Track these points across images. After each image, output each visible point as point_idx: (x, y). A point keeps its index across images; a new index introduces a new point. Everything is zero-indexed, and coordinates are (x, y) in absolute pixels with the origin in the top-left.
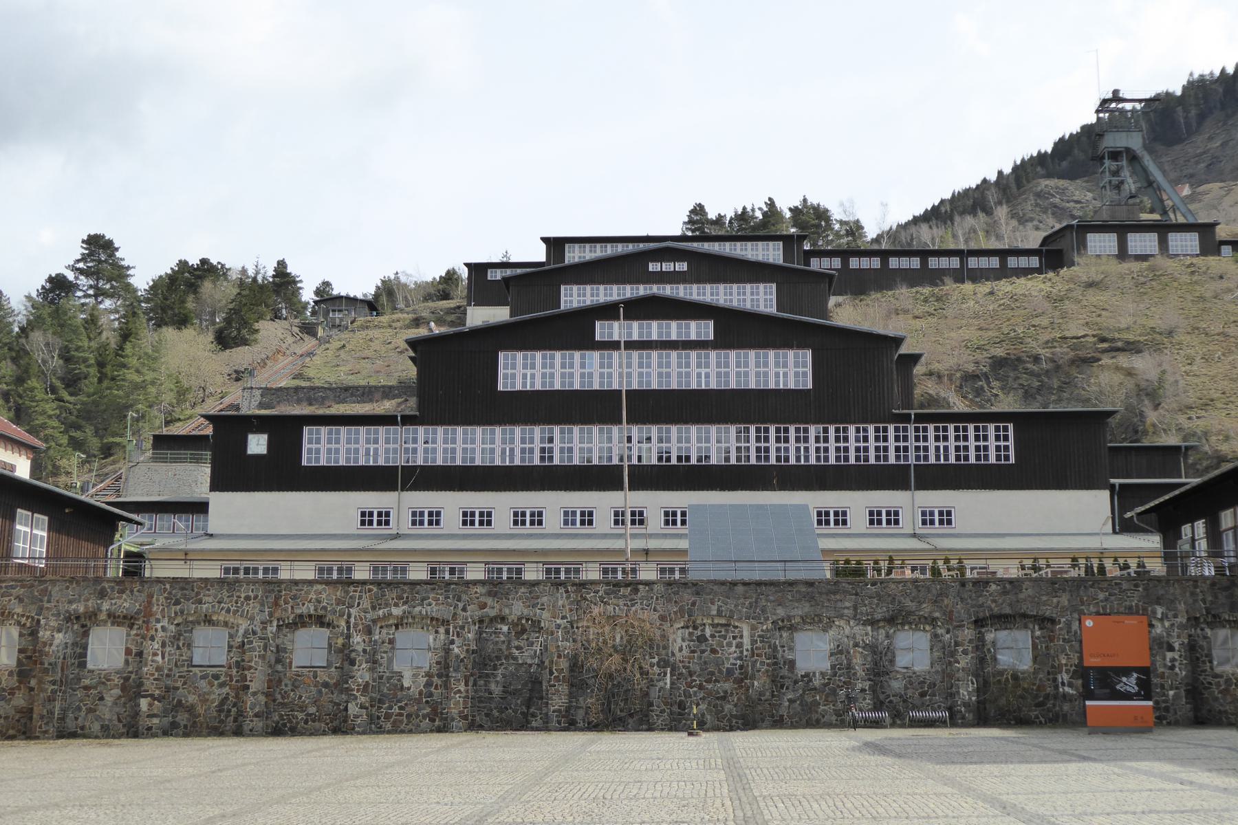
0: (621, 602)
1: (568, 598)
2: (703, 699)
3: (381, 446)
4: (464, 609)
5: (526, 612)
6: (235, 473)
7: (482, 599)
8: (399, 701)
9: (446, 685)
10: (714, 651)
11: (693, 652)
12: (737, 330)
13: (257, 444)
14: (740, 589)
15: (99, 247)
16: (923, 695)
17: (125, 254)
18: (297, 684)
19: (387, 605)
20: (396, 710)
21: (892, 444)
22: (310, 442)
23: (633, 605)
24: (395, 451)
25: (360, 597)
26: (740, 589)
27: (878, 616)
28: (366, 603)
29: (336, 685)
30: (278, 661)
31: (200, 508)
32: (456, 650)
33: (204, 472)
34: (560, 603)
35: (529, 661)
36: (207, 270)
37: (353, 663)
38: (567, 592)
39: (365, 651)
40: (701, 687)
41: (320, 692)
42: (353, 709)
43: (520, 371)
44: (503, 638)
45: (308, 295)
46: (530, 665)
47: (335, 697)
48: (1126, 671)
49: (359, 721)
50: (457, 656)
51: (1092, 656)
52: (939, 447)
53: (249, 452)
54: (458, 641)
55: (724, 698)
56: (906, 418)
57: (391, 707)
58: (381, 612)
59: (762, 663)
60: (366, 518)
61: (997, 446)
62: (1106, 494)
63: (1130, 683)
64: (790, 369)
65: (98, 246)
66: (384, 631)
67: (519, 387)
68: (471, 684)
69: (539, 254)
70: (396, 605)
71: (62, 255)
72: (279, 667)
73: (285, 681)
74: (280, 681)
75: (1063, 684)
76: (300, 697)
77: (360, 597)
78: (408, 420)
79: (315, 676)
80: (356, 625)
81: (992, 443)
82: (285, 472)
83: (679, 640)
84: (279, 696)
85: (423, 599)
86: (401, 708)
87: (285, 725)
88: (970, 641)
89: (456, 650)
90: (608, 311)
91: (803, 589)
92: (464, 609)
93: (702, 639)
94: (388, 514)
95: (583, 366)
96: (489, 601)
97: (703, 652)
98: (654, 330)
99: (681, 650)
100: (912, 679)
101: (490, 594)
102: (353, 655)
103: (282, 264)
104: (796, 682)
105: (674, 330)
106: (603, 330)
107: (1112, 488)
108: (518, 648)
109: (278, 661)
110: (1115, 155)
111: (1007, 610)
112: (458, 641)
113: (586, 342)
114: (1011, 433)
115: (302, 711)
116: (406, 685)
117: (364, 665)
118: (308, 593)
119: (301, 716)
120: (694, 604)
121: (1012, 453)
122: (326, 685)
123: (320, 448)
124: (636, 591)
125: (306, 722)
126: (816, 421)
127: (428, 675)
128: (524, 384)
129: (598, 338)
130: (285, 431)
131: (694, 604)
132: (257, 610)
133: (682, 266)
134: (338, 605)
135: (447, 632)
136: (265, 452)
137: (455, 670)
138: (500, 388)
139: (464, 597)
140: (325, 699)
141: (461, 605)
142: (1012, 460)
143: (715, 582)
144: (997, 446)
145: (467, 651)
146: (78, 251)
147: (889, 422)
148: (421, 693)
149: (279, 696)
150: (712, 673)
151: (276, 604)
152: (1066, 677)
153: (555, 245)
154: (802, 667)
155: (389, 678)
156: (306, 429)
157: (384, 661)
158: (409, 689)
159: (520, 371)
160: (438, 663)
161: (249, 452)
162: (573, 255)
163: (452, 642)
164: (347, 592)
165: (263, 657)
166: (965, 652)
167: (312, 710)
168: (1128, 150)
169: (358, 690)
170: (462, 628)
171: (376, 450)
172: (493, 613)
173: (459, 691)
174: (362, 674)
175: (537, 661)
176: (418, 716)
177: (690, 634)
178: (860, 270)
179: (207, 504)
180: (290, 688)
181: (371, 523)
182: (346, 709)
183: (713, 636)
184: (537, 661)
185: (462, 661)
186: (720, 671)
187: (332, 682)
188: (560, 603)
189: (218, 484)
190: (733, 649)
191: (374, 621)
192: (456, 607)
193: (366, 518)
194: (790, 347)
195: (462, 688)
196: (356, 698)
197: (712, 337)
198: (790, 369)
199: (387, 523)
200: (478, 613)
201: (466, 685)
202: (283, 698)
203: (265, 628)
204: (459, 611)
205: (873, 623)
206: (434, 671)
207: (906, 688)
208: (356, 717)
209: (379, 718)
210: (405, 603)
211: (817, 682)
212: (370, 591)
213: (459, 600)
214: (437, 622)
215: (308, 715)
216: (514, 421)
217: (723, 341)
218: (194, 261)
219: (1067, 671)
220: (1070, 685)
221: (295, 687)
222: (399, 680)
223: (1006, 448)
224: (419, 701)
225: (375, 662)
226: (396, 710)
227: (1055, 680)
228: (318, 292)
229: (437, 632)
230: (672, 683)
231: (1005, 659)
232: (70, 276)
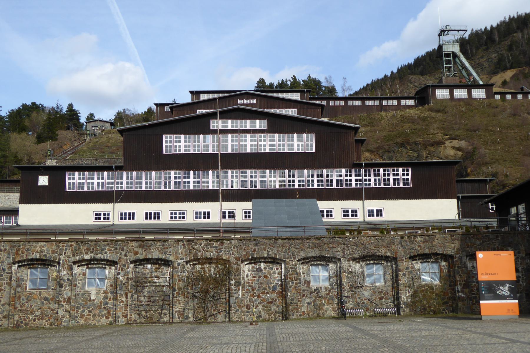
0: (214, 250)
1: (184, 248)
2: (260, 303)
3: (105, 181)
4: (126, 255)
5: (161, 256)
6: (33, 196)
7: (136, 249)
8: (88, 307)
9: (116, 298)
10: (266, 277)
11: (254, 277)
12: (279, 125)
14: (280, 241)
16: (381, 299)
18: (29, 298)
19: (81, 253)
20: (86, 312)
21: (353, 178)
22: (70, 179)
23: (221, 252)
24: (112, 183)
25: (66, 249)
26: (280, 241)
27: (356, 256)
28: (69, 253)
29: (52, 299)
30: (19, 286)
31: (15, 212)
32: (121, 278)
33: (16, 196)
34: (180, 251)
35: (162, 284)
36: (35, 107)
37: (61, 286)
38: (184, 245)
39: (68, 279)
40: (259, 297)
41: (43, 303)
42: (61, 312)
43: (173, 144)
44: (148, 271)
45: (83, 120)
46: (163, 286)
47: (52, 306)
48: (502, 283)
49: (64, 319)
50: (121, 282)
51: (482, 274)
53: (39, 184)
54: (122, 274)
55: (271, 302)
56: (359, 166)
57: (83, 311)
58: (78, 258)
59: (293, 283)
60: (98, 216)
62: (455, 201)
63: (505, 290)
64: (304, 143)
66: (80, 268)
67: (173, 152)
68: (129, 297)
69: (188, 99)
70: (87, 253)
72: (19, 289)
73: (23, 297)
74: (19, 297)
75: (458, 291)
76: (31, 306)
77: (66, 249)
78: (119, 168)
79: (40, 294)
80: (63, 265)
81: (401, 177)
82: (57, 194)
83: (246, 271)
84: (18, 306)
85: (102, 250)
86: (89, 311)
87: (22, 322)
88: (407, 269)
89: (121, 278)
91: (315, 241)
92: (126, 255)
93: (259, 270)
94: (108, 214)
95: (204, 141)
96: (140, 250)
97: (260, 277)
98: (239, 124)
99: (247, 276)
100: (374, 290)
101: (140, 246)
102: (62, 282)
103: (71, 106)
104: (311, 293)
105: (248, 124)
106: (214, 124)
107: (458, 199)
108: (156, 277)
109: (19, 286)
110: (448, 55)
111: (427, 251)
112: (122, 274)
113: (206, 130)
114: (410, 172)
115: (32, 314)
116: (93, 298)
117: (68, 288)
118: (35, 247)
119: (31, 317)
120: (254, 250)
122: (46, 299)
123: (74, 182)
124: (222, 243)
125: (34, 320)
126: (318, 167)
127: (106, 292)
128: (176, 151)
129: (211, 128)
130: (57, 174)
131: (254, 250)
132: (5, 257)
134: (53, 253)
135: (116, 269)
136: (47, 184)
137: (120, 290)
138: (164, 152)
139: (125, 248)
140: (45, 307)
141: (123, 253)
142: (410, 185)
143: (266, 238)
145: (127, 279)
147: (352, 168)
148: (101, 303)
149: (18, 306)
150: (265, 289)
151: (17, 254)
152: (459, 287)
153: (195, 94)
154: (314, 285)
155: (83, 295)
156: (67, 173)
157: (80, 285)
158: (94, 300)
159: (175, 144)
160: (111, 286)
161: (39, 184)
162: (204, 97)
163: (118, 274)
164: (58, 247)
165: (9, 284)
166: (404, 275)
167: (38, 313)
168: (453, 52)
169: (64, 302)
170: (125, 266)
171: (103, 183)
172: (142, 257)
173: (123, 301)
174: (66, 293)
175: (167, 284)
176: (99, 316)
177: (253, 267)
178: (335, 106)
179: (18, 211)
180: (25, 301)
181: (100, 219)
182: (57, 313)
183: (265, 268)
184: (167, 284)
185: (124, 284)
186: (269, 288)
187: (50, 297)
188: (180, 251)
189: (23, 201)
190: (277, 275)
191: (74, 263)
192: (121, 254)
193: (98, 216)
194: (304, 132)
195: (124, 299)
196: (63, 306)
197: (266, 128)
199: (108, 219)
200: (133, 258)
201: (127, 297)
202: (21, 306)
203: (11, 267)
204: (123, 256)
205: (354, 260)
206: (109, 290)
207: (372, 295)
208: (63, 317)
209: (77, 317)
210: (92, 252)
211: (323, 293)
212: (72, 245)
213: (123, 250)
214: (112, 263)
215: (36, 316)
216: (171, 168)
217: (272, 129)
218: (29, 103)
219: (461, 284)
220: (462, 292)
221: (28, 300)
222: (89, 296)
223: (408, 179)
224: (100, 307)
225: (75, 286)
226: (86, 312)
227: (454, 289)
228: (88, 118)
229: (110, 268)
230: (243, 295)
231: (426, 278)
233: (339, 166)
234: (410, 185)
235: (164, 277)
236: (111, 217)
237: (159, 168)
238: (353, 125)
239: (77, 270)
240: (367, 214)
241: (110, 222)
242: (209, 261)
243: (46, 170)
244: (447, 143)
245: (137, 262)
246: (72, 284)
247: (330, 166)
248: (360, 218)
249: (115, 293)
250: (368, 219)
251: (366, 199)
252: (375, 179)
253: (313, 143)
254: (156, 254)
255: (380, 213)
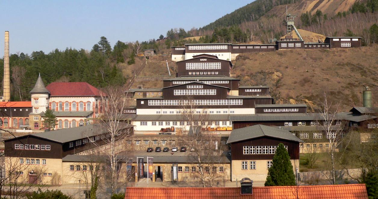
13: (142, 102)
15: (104, 40)
17: (109, 40)
52: (233, 103)
56: (228, 99)
60: (157, 112)
61: (240, 102)
62: (254, 109)
64: (213, 92)
65: (104, 40)
71: (97, 41)
82: (146, 106)
90: (188, 84)
107: (255, 108)
113: (186, 88)
114: (242, 101)
121: (242, 103)
123: (151, 103)
130: (146, 100)
133: (206, 60)
142: (242, 104)
144: (240, 102)
146: (99, 40)
168: (291, 25)
178: (242, 49)
193: (157, 112)
197: (203, 88)
198: (213, 92)
214: (166, 140)
217: (204, 88)
232: (98, 44)
233: (223, 99)
234: (242, 104)
235: (174, 142)
236: (161, 112)
237: (173, 99)
238: (226, 87)
239: (161, 141)
240: (230, 112)
241: (160, 114)
242: (181, 140)
243: (143, 100)
244: (275, 73)
245: (170, 140)
246: (160, 143)
247: (220, 99)
248: (228, 113)
249: (167, 145)
250: (230, 114)
251: (230, 108)
252: (233, 103)
253: (216, 92)
254: (173, 139)
255: (233, 112)
